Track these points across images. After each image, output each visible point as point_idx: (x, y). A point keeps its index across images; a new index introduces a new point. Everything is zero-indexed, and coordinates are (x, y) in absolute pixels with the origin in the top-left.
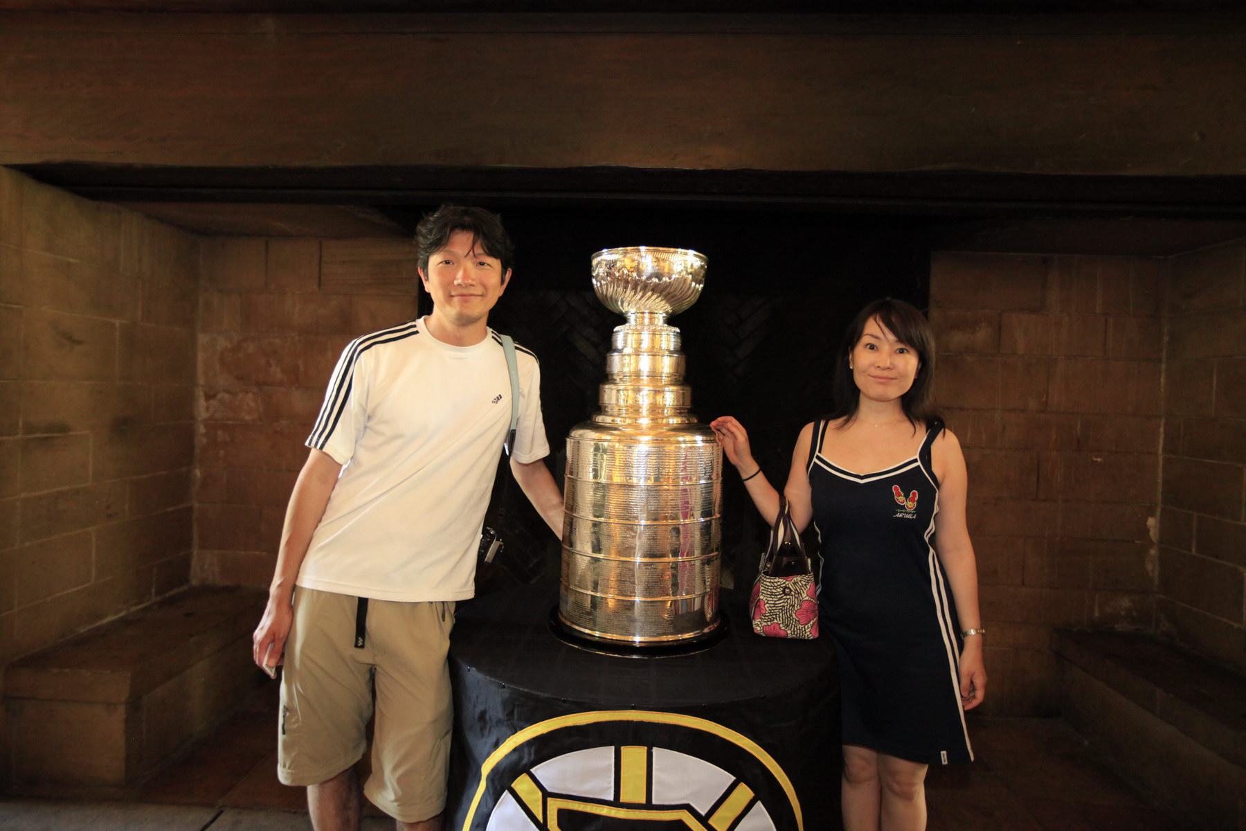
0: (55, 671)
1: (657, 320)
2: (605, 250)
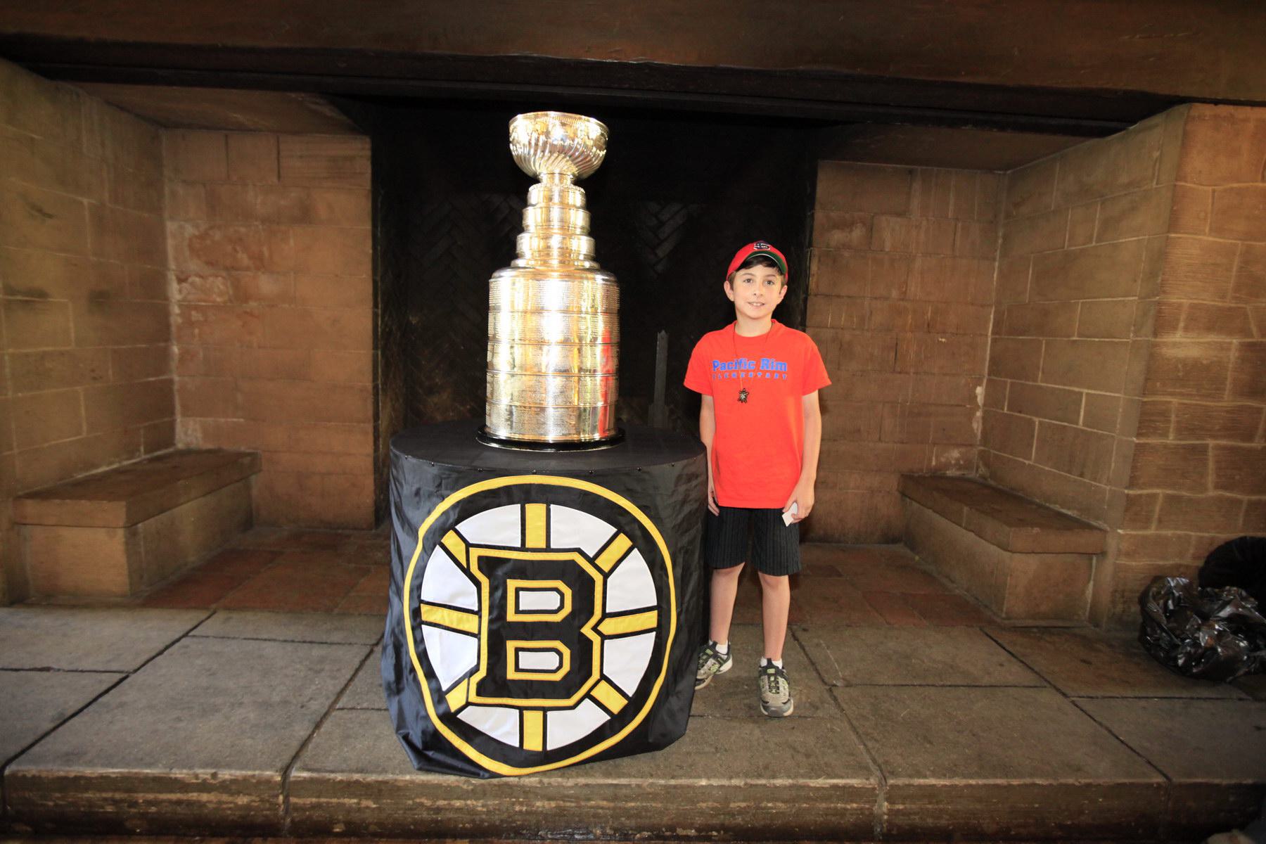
0: (57, 501)
1: (565, 181)
2: (520, 117)
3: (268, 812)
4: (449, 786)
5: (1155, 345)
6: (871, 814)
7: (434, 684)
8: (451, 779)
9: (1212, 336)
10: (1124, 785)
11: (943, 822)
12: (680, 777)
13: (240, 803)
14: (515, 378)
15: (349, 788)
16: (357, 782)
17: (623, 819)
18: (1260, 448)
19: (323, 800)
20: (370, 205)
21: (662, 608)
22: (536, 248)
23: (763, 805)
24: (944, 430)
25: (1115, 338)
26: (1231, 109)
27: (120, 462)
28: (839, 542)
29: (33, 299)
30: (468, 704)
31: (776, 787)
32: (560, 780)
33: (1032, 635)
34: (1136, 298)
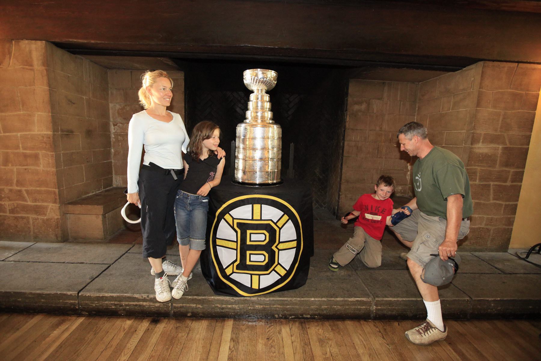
0: (80, 205)
3: (166, 309)
4: (226, 300)
5: (472, 148)
6: (370, 310)
8: (227, 298)
9: (492, 145)
10: (456, 300)
11: (394, 313)
12: (305, 298)
13: (156, 306)
15: (193, 301)
16: (196, 299)
17: (285, 312)
18: (509, 185)
19: (184, 305)
20: (184, 97)
21: (298, 240)
22: (253, 116)
23: (333, 307)
26: (499, 63)
27: (96, 192)
29: (70, 133)
32: (264, 298)
34: (465, 131)
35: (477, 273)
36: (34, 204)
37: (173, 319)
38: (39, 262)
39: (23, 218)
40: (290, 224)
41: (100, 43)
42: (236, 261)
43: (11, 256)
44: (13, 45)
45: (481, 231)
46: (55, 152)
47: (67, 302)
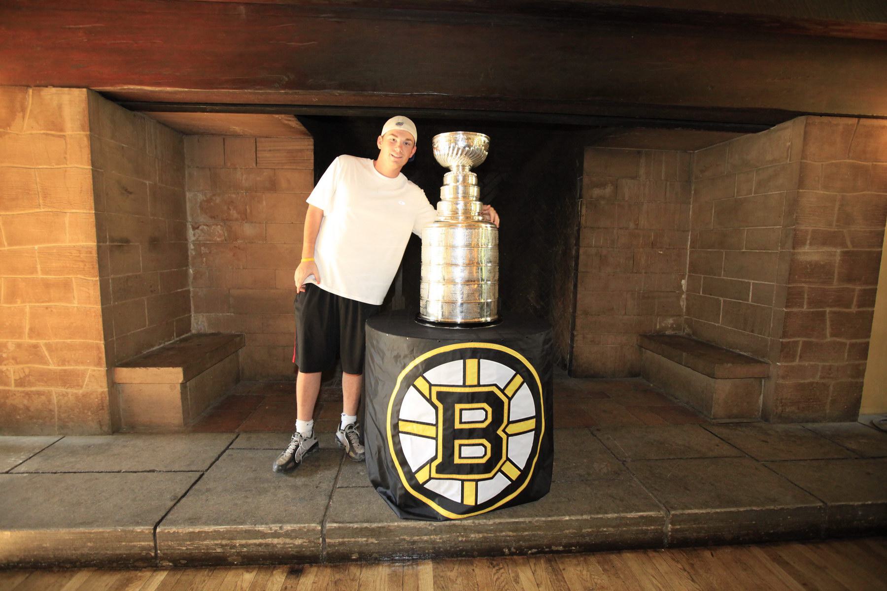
1: (466, 170)
3: (313, 549)
4: (420, 528)
5: (794, 254)
7: (406, 469)
8: (421, 524)
9: (825, 248)
11: (702, 535)
12: (553, 516)
13: (297, 544)
14: (444, 286)
15: (361, 532)
16: (366, 528)
17: (521, 542)
18: (854, 312)
19: (346, 540)
21: (538, 417)
23: (601, 530)
24: (664, 307)
25: (769, 250)
26: (829, 118)
28: (603, 377)
30: (430, 478)
31: (609, 519)
32: (485, 521)
33: (730, 427)
35: (821, 459)
36: (60, 368)
37: (326, 567)
38: (75, 473)
39: (39, 394)
40: (526, 390)
41: (181, 92)
42: (435, 458)
43: (21, 464)
44: (29, 95)
45: (815, 387)
46: (100, 276)
47: (135, 546)
